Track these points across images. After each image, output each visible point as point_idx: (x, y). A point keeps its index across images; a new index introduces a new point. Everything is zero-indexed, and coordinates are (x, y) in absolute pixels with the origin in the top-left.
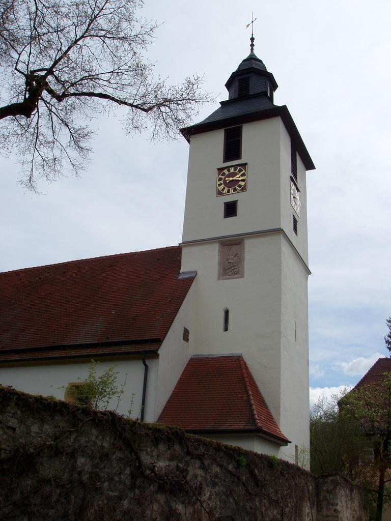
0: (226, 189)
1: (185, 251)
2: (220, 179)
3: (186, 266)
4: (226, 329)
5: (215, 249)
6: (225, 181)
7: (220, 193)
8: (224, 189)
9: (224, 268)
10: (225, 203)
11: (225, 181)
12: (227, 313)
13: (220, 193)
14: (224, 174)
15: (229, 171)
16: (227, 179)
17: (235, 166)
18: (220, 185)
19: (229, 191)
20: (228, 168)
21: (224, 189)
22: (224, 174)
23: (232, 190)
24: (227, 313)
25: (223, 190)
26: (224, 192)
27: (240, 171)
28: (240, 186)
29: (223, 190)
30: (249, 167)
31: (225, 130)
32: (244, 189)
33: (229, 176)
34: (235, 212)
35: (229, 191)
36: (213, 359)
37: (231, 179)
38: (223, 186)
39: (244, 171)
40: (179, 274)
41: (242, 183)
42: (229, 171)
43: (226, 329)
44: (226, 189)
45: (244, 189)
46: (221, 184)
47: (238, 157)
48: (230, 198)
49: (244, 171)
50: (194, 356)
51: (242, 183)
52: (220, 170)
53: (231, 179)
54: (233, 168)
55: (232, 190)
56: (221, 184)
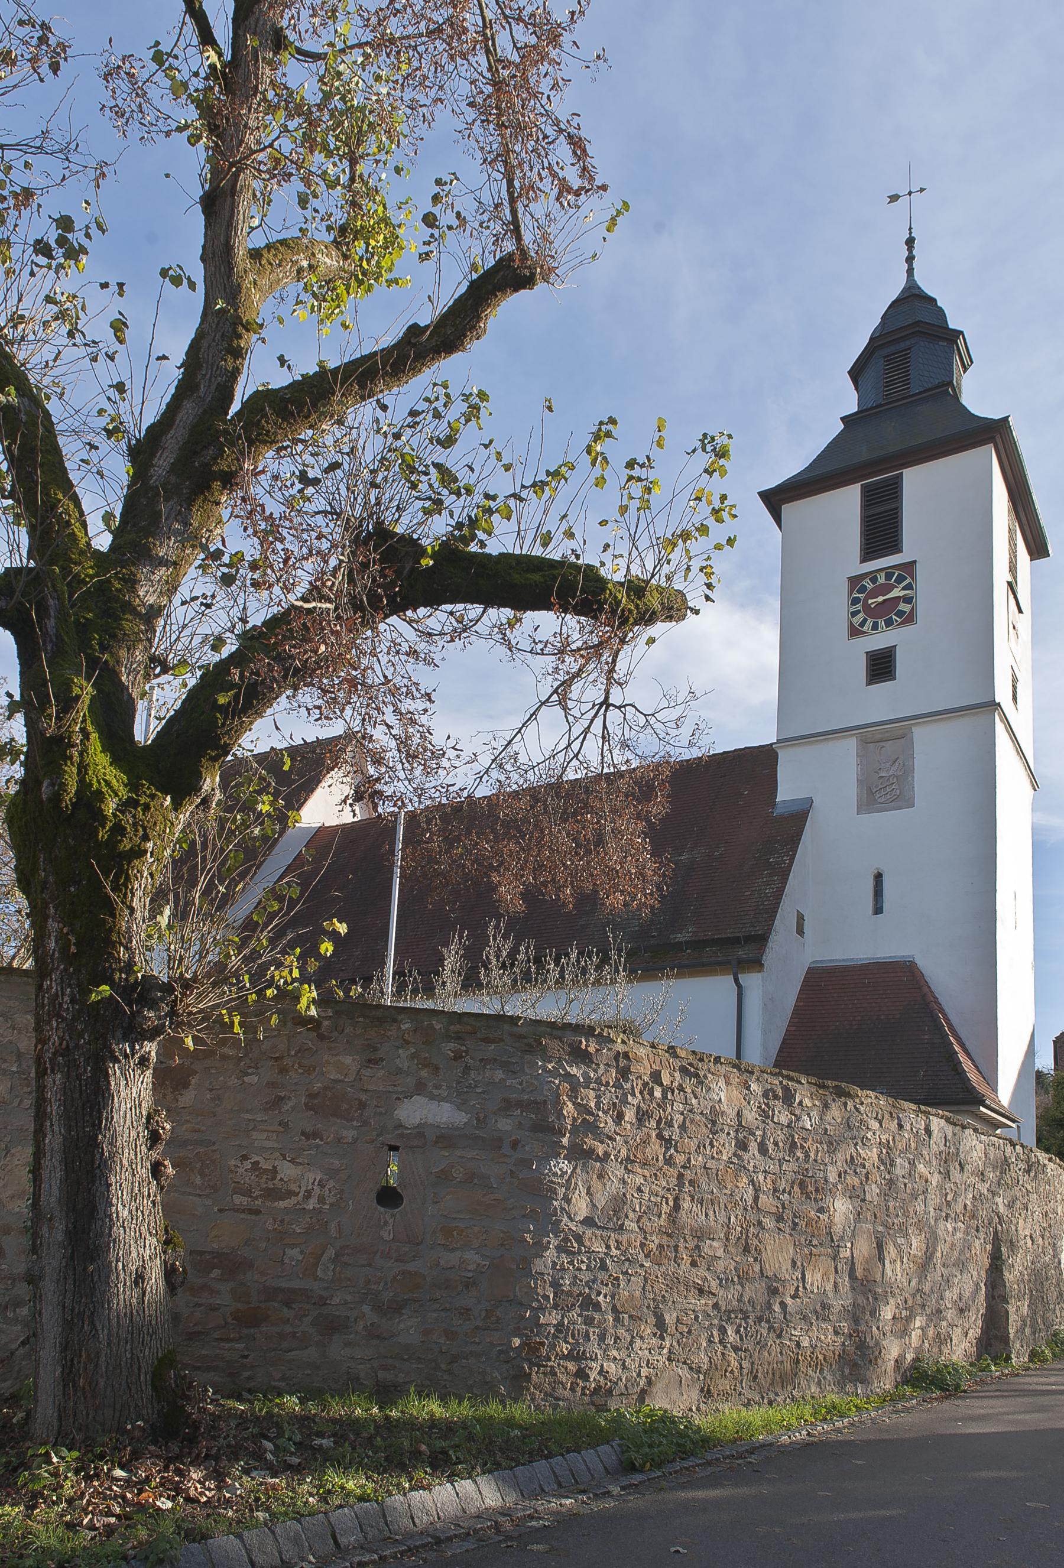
0: (870, 623)
1: (783, 756)
2: (855, 601)
3: (787, 791)
4: (878, 910)
5: (851, 745)
6: (866, 607)
7: (855, 632)
8: (864, 621)
9: (869, 789)
10: (867, 653)
11: (866, 607)
12: (879, 877)
13: (855, 632)
14: (863, 589)
15: (874, 580)
16: (870, 601)
17: (888, 572)
18: (854, 614)
19: (875, 627)
20: (873, 576)
21: (864, 621)
22: (863, 589)
23: (882, 623)
24: (879, 877)
25: (862, 624)
26: (865, 629)
27: (900, 579)
28: (900, 614)
29: (862, 624)
30: (920, 570)
31: (866, 491)
32: (909, 619)
33: (874, 594)
34: (890, 672)
35: (875, 627)
36: (854, 967)
37: (881, 599)
38: (861, 616)
39: (909, 580)
40: (773, 804)
41: (904, 607)
42: (874, 580)
43: (878, 910)
44: (870, 623)
45: (909, 619)
46: (858, 612)
47: (894, 545)
48: (879, 641)
49: (909, 580)
50: (813, 962)
51: (904, 607)
52: (855, 582)
53: (881, 599)
54: (883, 574)
55: (882, 623)
56: (858, 612)
